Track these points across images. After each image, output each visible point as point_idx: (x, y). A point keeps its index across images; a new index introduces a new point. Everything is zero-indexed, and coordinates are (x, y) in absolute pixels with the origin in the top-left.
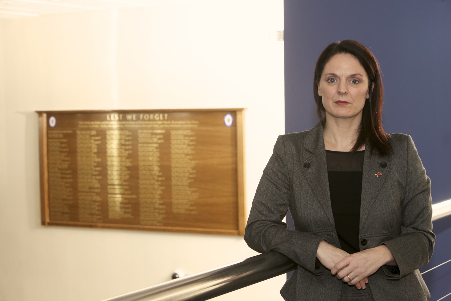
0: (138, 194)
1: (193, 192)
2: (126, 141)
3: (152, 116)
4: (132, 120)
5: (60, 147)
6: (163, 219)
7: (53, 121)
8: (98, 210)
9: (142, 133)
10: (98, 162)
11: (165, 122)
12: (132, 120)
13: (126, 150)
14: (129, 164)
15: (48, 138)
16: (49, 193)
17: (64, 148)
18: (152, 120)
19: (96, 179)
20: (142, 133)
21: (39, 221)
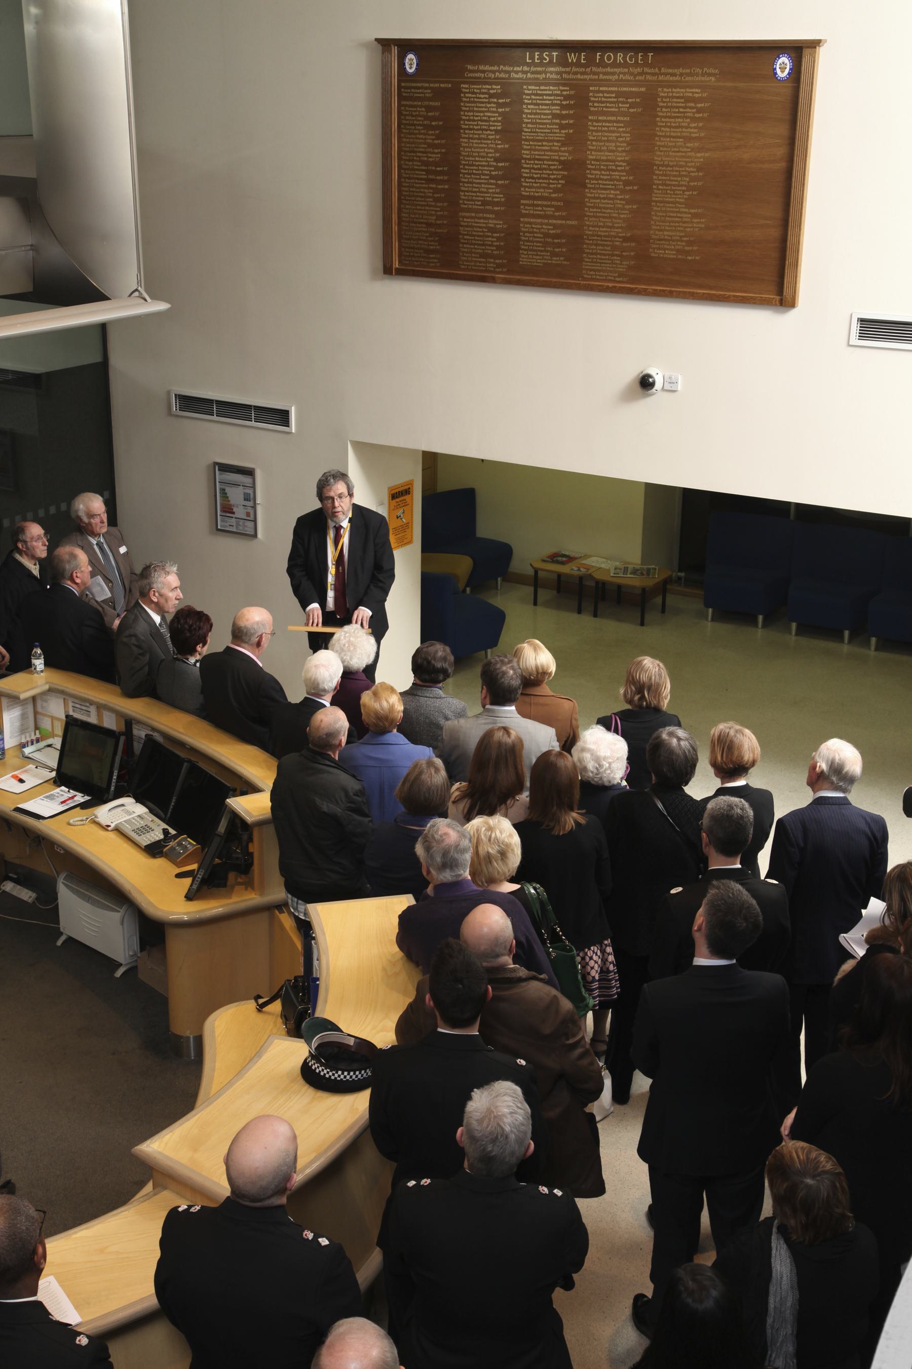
1: (695, 216)
3: (620, 56)
5: (426, 118)
7: (411, 62)
9: (599, 92)
11: (646, 70)
12: (578, 64)
13: (562, 127)
14: (565, 156)
15: (400, 97)
18: (620, 65)
19: (497, 186)
20: (599, 92)
21: (380, 265)
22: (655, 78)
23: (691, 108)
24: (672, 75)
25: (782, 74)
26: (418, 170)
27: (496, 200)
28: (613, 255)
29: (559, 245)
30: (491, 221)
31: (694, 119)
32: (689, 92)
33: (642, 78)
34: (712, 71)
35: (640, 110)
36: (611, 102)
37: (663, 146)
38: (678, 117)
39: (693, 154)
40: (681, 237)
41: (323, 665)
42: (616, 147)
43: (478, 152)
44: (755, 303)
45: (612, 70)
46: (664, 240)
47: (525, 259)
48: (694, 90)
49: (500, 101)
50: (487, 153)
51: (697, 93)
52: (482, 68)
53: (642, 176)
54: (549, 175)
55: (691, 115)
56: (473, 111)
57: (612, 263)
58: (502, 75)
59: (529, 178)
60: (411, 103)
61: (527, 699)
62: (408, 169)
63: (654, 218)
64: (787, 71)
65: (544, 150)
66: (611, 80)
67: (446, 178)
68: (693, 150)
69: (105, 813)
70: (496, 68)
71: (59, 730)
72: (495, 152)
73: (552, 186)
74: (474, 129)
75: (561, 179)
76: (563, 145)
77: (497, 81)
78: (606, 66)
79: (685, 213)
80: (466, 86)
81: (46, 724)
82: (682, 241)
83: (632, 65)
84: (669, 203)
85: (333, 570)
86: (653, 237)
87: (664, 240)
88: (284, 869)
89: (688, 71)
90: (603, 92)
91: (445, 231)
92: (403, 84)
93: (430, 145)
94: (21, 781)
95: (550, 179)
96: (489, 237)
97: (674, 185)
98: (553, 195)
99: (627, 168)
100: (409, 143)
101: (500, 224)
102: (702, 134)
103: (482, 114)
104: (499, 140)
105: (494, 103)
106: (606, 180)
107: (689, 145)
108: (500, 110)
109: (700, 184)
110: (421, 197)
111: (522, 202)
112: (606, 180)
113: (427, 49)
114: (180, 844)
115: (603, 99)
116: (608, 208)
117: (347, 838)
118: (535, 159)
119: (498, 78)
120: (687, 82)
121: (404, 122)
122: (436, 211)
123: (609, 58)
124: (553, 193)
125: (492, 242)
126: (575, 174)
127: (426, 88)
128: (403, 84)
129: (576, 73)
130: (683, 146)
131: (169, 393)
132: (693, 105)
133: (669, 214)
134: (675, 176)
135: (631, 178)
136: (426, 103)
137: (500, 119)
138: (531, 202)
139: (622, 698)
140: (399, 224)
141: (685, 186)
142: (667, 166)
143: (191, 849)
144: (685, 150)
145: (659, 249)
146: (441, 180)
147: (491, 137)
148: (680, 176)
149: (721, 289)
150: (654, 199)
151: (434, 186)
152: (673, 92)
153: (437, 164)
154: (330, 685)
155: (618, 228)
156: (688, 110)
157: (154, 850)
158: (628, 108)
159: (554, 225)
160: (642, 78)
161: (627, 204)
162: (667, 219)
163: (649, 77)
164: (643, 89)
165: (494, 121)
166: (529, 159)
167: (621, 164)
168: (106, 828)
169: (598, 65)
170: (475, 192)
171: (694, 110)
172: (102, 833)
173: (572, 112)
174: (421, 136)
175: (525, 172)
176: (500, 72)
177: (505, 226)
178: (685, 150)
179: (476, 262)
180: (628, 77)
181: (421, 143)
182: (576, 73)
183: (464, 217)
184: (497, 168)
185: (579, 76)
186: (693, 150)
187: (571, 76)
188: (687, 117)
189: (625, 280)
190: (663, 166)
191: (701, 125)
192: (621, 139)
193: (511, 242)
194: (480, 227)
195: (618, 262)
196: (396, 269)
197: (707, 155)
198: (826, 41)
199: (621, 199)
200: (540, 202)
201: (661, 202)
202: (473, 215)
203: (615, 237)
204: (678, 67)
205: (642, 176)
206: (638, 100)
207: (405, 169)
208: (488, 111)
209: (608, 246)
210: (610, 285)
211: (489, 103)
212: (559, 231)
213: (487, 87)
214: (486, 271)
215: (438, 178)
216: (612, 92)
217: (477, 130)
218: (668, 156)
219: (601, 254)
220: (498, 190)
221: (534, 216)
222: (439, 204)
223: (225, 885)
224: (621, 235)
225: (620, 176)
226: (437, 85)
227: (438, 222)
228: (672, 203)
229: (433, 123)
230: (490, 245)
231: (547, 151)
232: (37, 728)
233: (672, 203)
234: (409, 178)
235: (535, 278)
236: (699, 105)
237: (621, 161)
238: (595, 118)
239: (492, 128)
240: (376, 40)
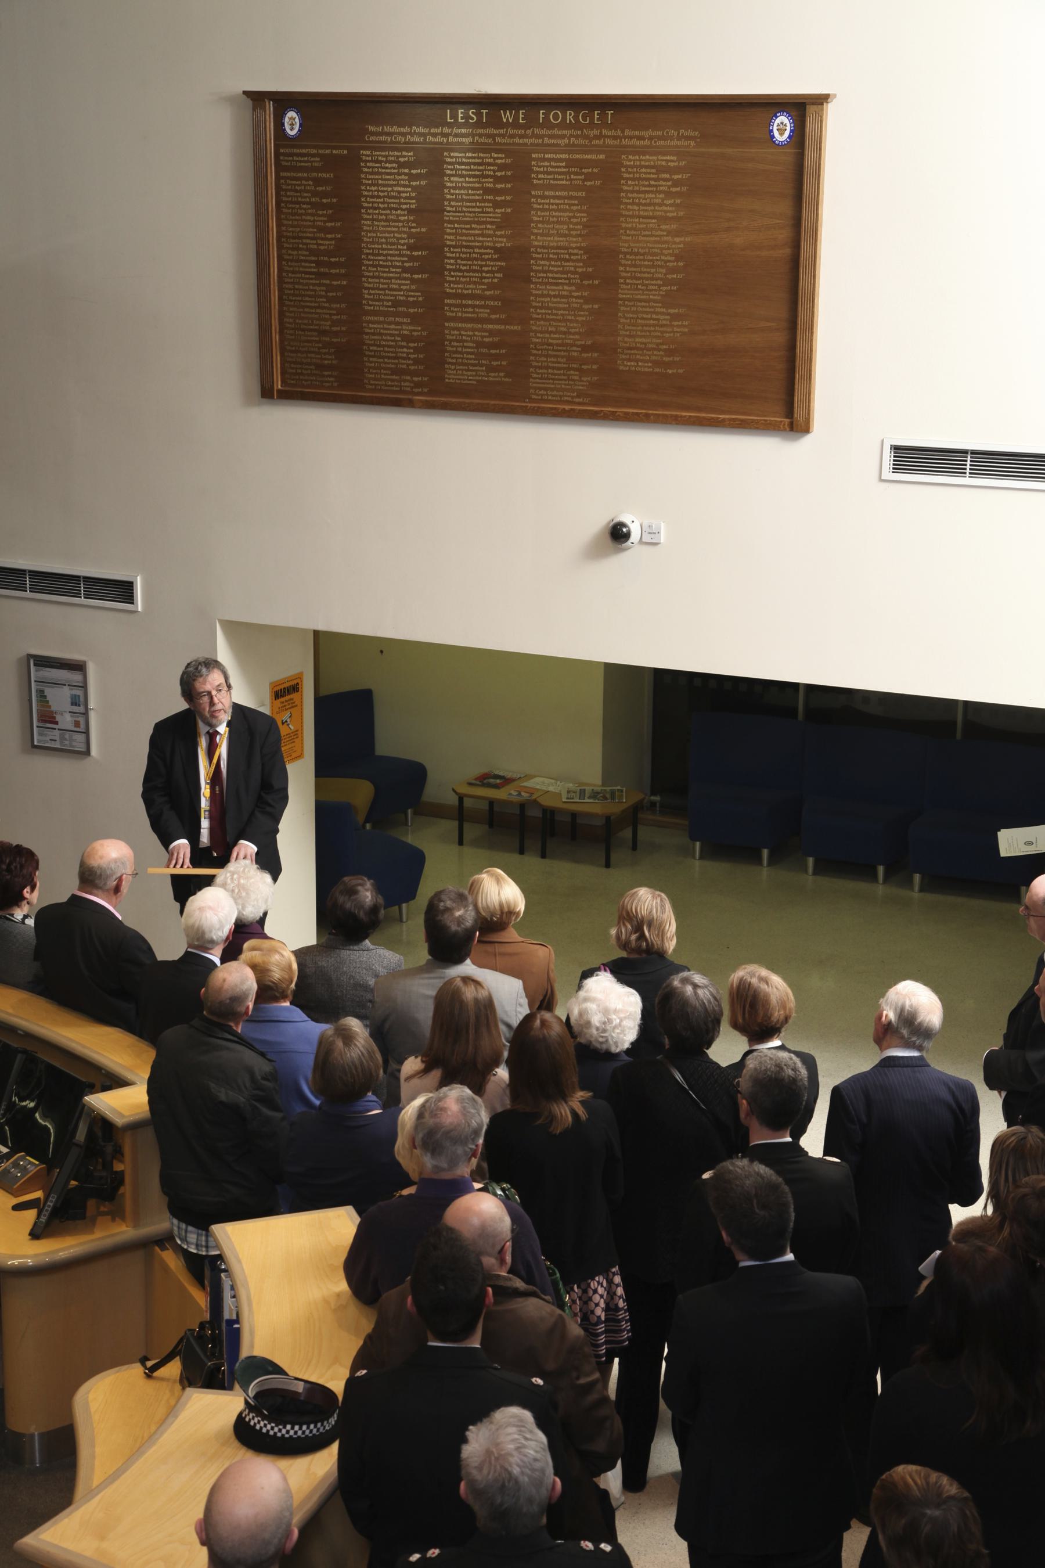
2: (497, 179)
5: (315, 194)
8: (416, 362)
9: (544, 159)
11: (605, 132)
12: (515, 124)
14: (503, 243)
15: (279, 167)
16: (281, 314)
18: (570, 126)
20: (544, 159)
24: (639, 138)
25: (781, 138)
26: (305, 261)
27: (411, 299)
28: (569, 369)
29: (497, 357)
30: (405, 327)
31: (669, 194)
32: (662, 160)
33: (601, 142)
35: (598, 183)
36: (560, 173)
37: (630, 229)
38: (648, 192)
39: (669, 238)
40: (658, 344)
41: (210, 908)
42: (569, 230)
43: (386, 238)
44: (757, 428)
45: (560, 132)
46: (637, 348)
47: (452, 376)
48: (668, 158)
49: (414, 172)
50: (398, 239)
51: (672, 161)
52: (387, 129)
54: (481, 266)
55: (666, 189)
56: (378, 185)
57: (569, 380)
58: (416, 139)
59: (454, 270)
60: (294, 174)
61: (489, 948)
62: (292, 261)
63: (623, 320)
64: (787, 133)
65: (474, 235)
66: (558, 145)
67: (343, 271)
68: (669, 233)
70: (406, 129)
72: (408, 238)
73: (485, 281)
74: (379, 208)
75: (497, 272)
76: (499, 227)
77: (408, 146)
78: (552, 127)
79: (663, 314)
80: (368, 152)
82: (659, 350)
84: (640, 301)
85: (201, 790)
86: (622, 345)
87: (637, 348)
88: (168, 1184)
89: (660, 133)
90: (549, 160)
91: (344, 340)
92: (282, 151)
93: (321, 229)
95: (482, 272)
96: (402, 347)
97: (647, 279)
98: (488, 293)
99: (585, 257)
100: (292, 226)
101: (417, 331)
102: (681, 214)
103: (390, 188)
104: (413, 222)
105: (405, 174)
106: (557, 272)
107: (664, 227)
108: (414, 183)
109: (680, 276)
110: (309, 296)
111: (446, 301)
112: (557, 272)
115: (550, 169)
117: (244, 1145)
118: (462, 246)
119: (409, 143)
120: (658, 147)
121: (284, 199)
122: (331, 314)
123: (556, 117)
124: (487, 290)
125: (408, 354)
126: (515, 266)
127: (313, 155)
128: (282, 151)
129: (512, 136)
132: (667, 176)
133: (640, 315)
134: (647, 266)
135: (590, 270)
136: (315, 174)
137: (413, 194)
138: (459, 302)
139: (613, 941)
140: (281, 332)
141: (661, 279)
144: (659, 233)
145: (629, 360)
146: (336, 274)
147: (402, 218)
148: (653, 266)
150: (621, 296)
151: (328, 282)
152: (640, 160)
153: (329, 253)
154: (220, 934)
155: (574, 334)
156: (662, 183)
158: (584, 180)
160: (601, 142)
161: (587, 302)
162: (639, 321)
163: (608, 141)
164: (602, 157)
165: (405, 198)
166: (454, 247)
167: (576, 251)
169: (542, 126)
170: (384, 289)
171: (670, 183)
173: (509, 186)
174: (308, 218)
175: (449, 264)
176: (412, 134)
177: (425, 333)
178: (659, 233)
179: (386, 380)
181: (309, 227)
182: (512, 136)
183: (369, 322)
184: (412, 259)
185: (517, 140)
186: (669, 233)
187: (506, 140)
188: (660, 192)
189: (586, 400)
190: (631, 254)
191: (678, 201)
192: (575, 220)
194: (391, 335)
195: (576, 378)
196: (278, 391)
197: (688, 239)
198: (835, 96)
199: (577, 297)
200: (470, 302)
201: (629, 300)
202: (381, 319)
203: (572, 345)
204: (646, 129)
205: (602, 268)
206: (596, 170)
207: (288, 261)
208: (397, 185)
209: (562, 357)
210: (567, 407)
211: (399, 174)
212: (496, 339)
213: (395, 153)
214: (401, 392)
215: (333, 271)
217: (384, 209)
218: (638, 241)
219: (553, 368)
220: (414, 287)
222: (335, 306)
224: (579, 343)
225: (575, 267)
226: (328, 151)
227: (334, 329)
228: (645, 301)
229: (325, 201)
230: (404, 358)
231: (478, 235)
233: (645, 301)
234: (293, 272)
235: (467, 401)
236: (676, 177)
237: (577, 248)
238: (540, 193)
239: (404, 207)
240: (245, 93)
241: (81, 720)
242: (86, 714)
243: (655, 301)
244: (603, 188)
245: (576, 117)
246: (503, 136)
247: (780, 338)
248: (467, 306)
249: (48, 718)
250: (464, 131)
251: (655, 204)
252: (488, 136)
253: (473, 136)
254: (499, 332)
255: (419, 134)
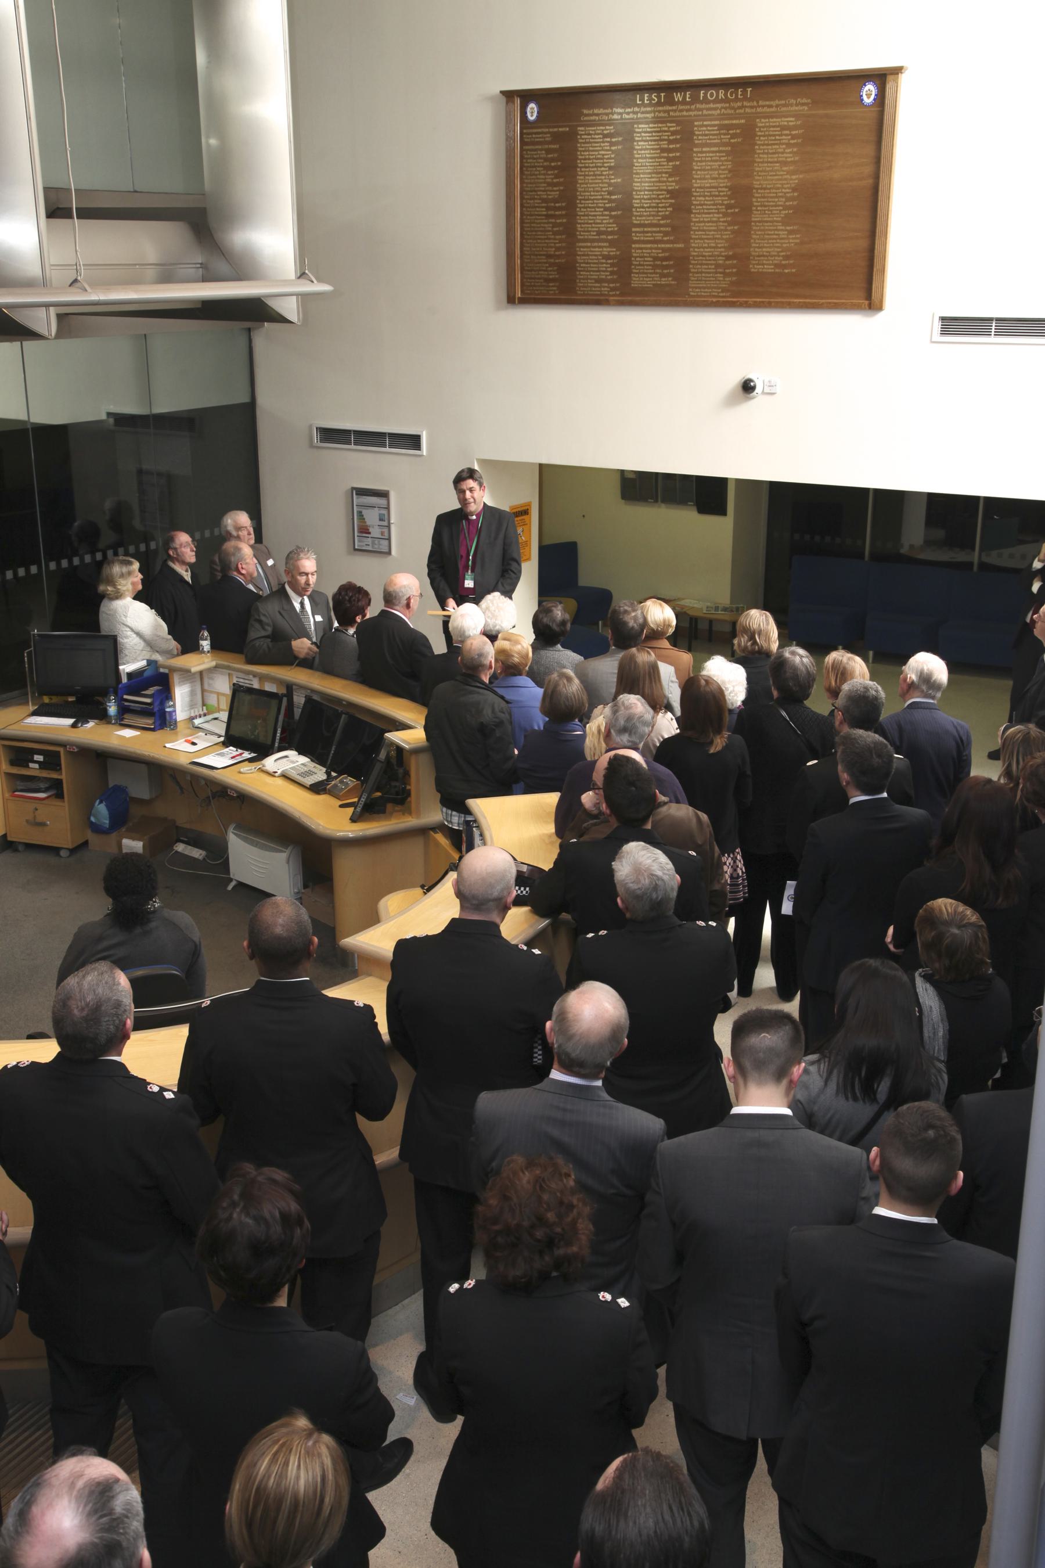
0: (687, 241)
1: (791, 232)
2: (670, 142)
4: (684, 102)
5: (546, 160)
6: (732, 283)
7: (532, 111)
8: (612, 273)
9: (703, 126)
10: (615, 185)
11: (745, 103)
12: (684, 102)
14: (673, 186)
15: (523, 143)
17: (553, 160)
18: (722, 101)
19: (611, 217)
20: (703, 126)
22: (754, 110)
23: (786, 135)
25: (868, 100)
28: (716, 273)
31: (789, 145)
33: (742, 111)
34: (805, 101)
35: (739, 140)
47: (636, 281)
51: (791, 121)
53: (741, 200)
68: (788, 172)
69: (270, 763)
70: (609, 111)
71: (225, 704)
76: (671, 175)
78: (709, 102)
81: (212, 700)
83: (732, 101)
84: (767, 222)
90: (706, 126)
93: (549, 184)
94: (194, 744)
102: (797, 158)
109: (795, 203)
113: (547, 98)
114: (341, 782)
116: (709, 233)
123: (712, 96)
130: (778, 172)
131: (311, 427)
136: (546, 146)
142: (765, 189)
143: (351, 785)
148: (776, 197)
149: (815, 297)
153: (555, 201)
157: (317, 788)
159: (662, 249)
163: (748, 110)
164: (743, 121)
168: (272, 774)
169: (702, 102)
172: (269, 780)
180: (729, 111)
184: (610, 201)
185: (685, 113)
186: (788, 172)
187: (677, 114)
190: (761, 189)
193: (623, 265)
205: (741, 200)
216: (714, 126)
221: (644, 242)
223: (384, 812)
226: (556, 130)
232: (204, 704)
234: (531, 215)
236: (794, 132)
238: (699, 149)
240: (501, 92)
241: (386, 530)
242: (389, 527)
243: (777, 222)
244: (743, 144)
245: (726, 95)
246: (675, 111)
247: (863, 243)
248: (648, 232)
249: (364, 530)
250: (649, 109)
251: (778, 153)
252: (665, 111)
253: (654, 112)
254: (669, 250)
255: (620, 113)
